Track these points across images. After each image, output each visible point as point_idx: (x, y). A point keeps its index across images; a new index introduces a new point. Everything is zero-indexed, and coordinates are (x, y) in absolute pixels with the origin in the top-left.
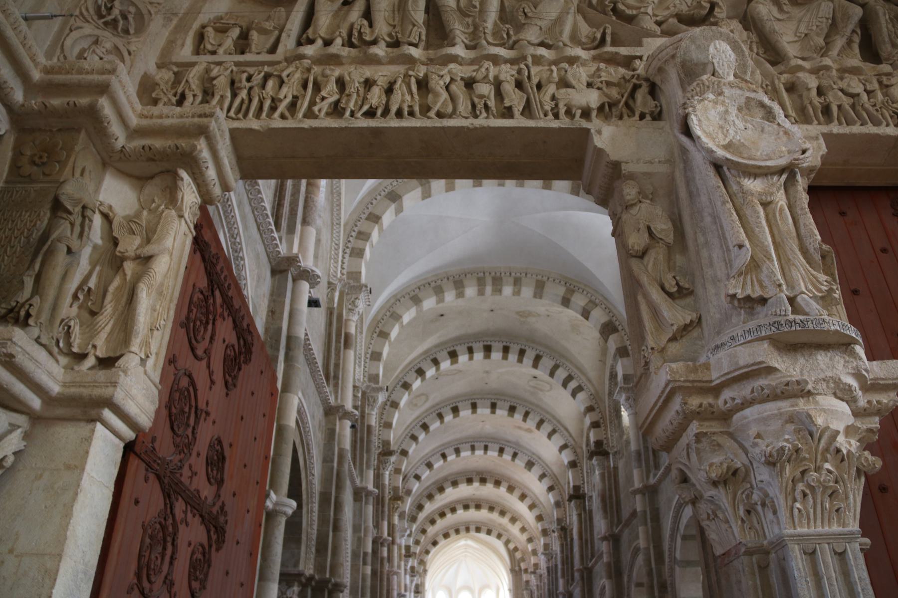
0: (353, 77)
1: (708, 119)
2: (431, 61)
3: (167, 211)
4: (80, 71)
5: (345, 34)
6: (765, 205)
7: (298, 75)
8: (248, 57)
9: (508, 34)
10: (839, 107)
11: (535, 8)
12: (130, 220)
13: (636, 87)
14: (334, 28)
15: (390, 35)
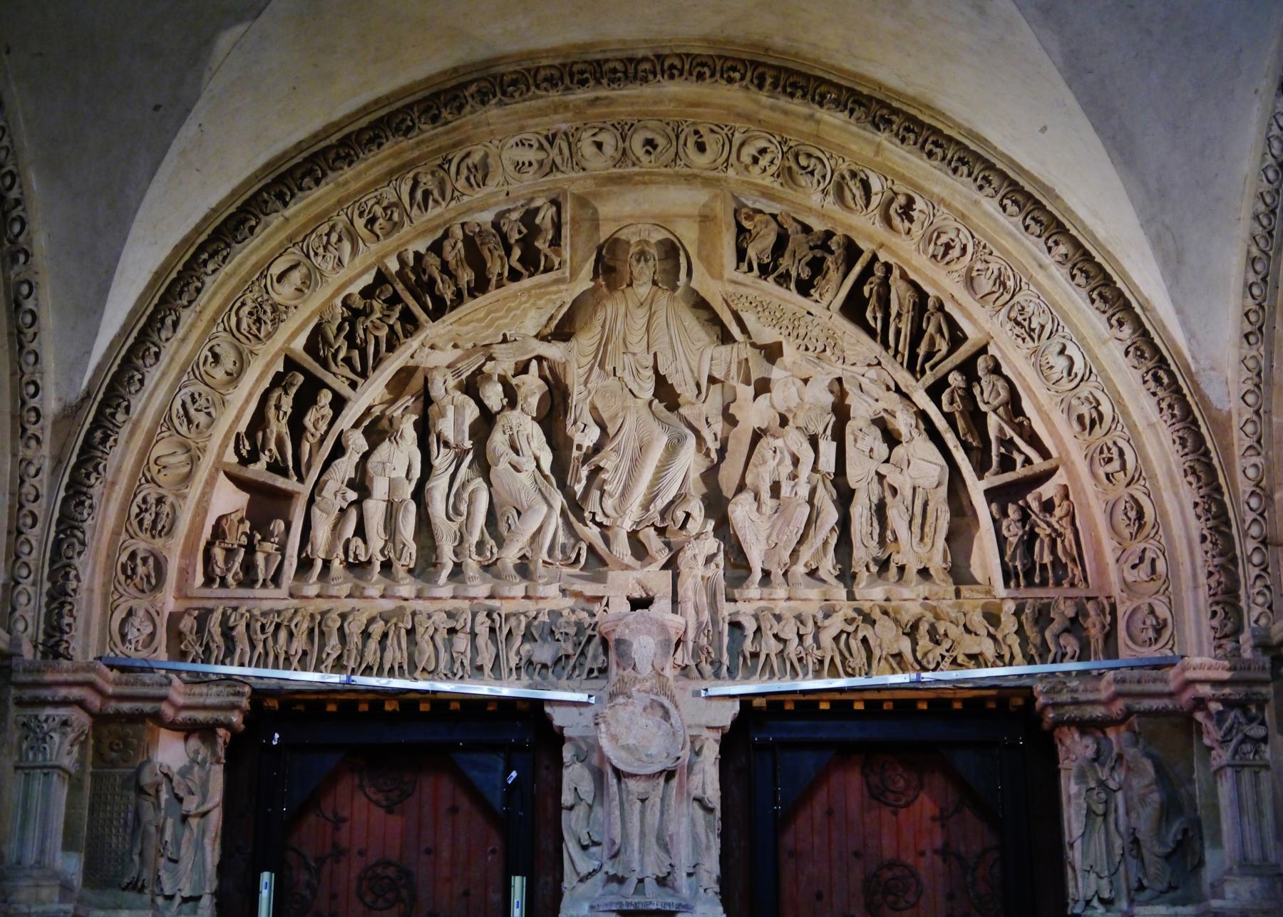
0: (352, 630)
1: (617, 720)
2: (418, 597)
3: (213, 767)
4: (144, 684)
5: (342, 556)
6: (643, 801)
7: (305, 625)
8: (258, 592)
9: (492, 553)
10: (768, 655)
11: (519, 513)
12: (185, 772)
13: (591, 638)
14: (331, 549)
15: (382, 551)
